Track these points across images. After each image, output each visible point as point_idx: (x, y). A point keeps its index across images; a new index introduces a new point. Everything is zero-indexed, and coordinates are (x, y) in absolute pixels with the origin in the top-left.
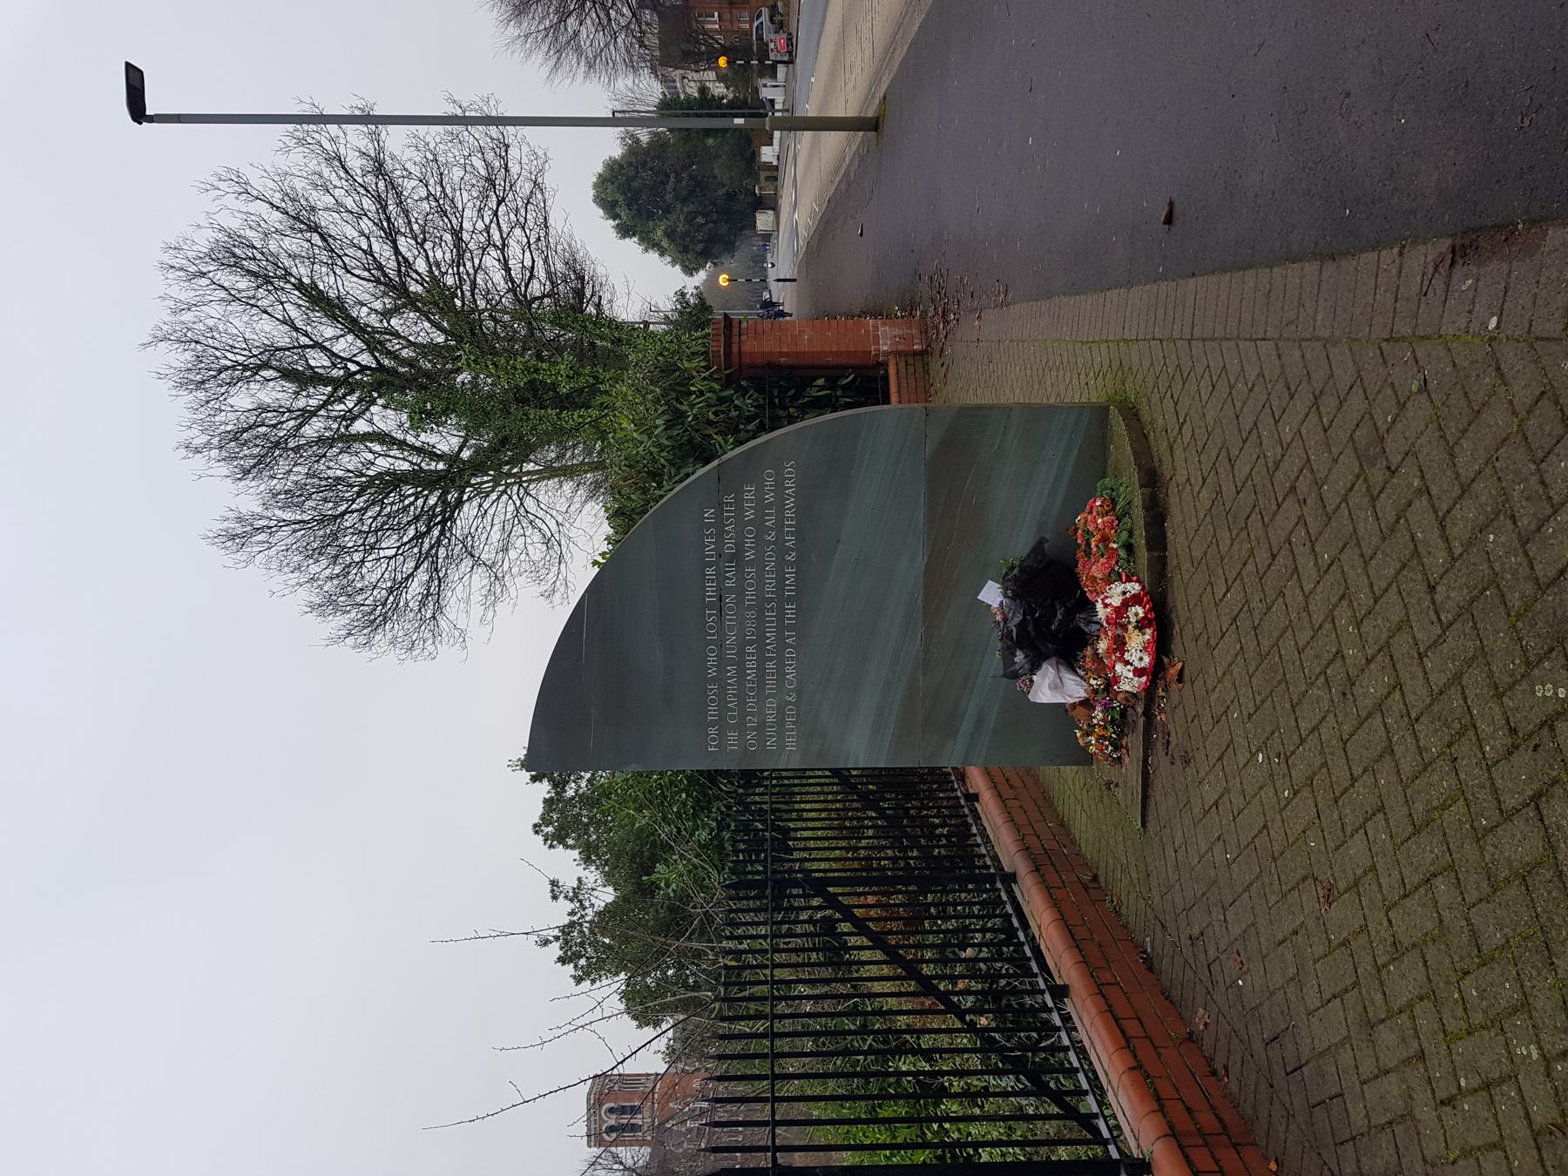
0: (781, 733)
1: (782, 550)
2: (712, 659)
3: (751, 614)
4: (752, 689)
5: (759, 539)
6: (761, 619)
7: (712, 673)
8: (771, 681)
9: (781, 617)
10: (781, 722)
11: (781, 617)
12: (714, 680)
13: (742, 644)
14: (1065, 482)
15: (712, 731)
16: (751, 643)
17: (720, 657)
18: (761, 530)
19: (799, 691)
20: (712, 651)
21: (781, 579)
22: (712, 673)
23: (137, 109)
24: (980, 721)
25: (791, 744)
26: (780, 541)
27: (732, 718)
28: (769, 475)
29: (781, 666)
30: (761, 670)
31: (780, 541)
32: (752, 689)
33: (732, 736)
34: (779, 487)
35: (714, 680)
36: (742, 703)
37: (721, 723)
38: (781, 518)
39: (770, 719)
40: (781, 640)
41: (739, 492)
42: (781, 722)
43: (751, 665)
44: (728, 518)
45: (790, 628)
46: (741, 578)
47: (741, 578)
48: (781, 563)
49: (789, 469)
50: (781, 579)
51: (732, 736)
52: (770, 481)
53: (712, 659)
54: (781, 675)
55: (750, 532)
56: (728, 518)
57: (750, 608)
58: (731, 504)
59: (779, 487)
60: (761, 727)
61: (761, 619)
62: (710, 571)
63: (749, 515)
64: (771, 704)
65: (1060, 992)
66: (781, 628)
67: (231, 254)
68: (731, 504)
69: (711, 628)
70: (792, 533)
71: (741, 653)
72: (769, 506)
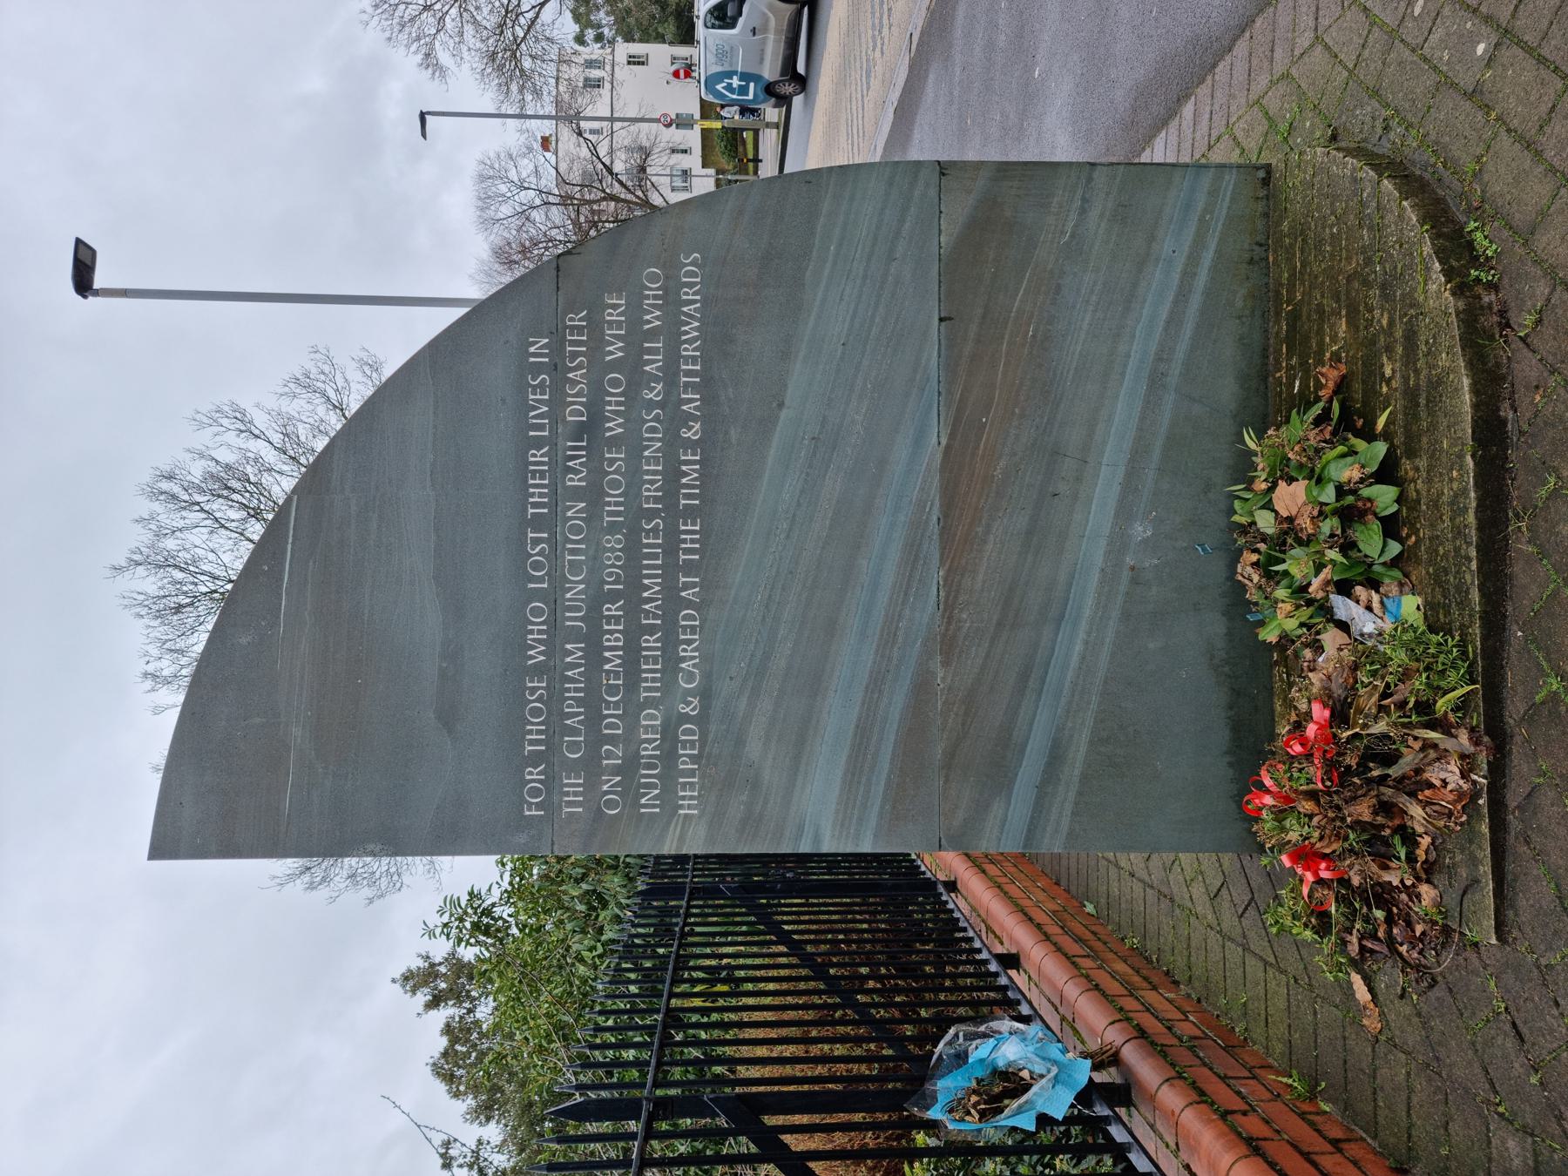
1: (675, 420)
2: (537, 628)
3: (614, 542)
4: (613, 690)
6: (633, 551)
7: (536, 655)
8: (650, 673)
9: (671, 549)
10: (669, 755)
11: (671, 549)
12: (539, 671)
13: (597, 599)
14: (1196, 301)
16: (613, 597)
17: (553, 623)
19: (705, 694)
20: (537, 612)
21: (673, 475)
22: (536, 655)
23: (83, 280)
24: (1056, 757)
26: (670, 403)
27: (574, 747)
28: (653, 278)
31: (670, 403)
33: (573, 784)
34: (671, 300)
35: (539, 671)
36: (594, 719)
37: (548, 757)
39: (648, 751)
40: (671, 591)
41: (596, 309)
42: (669, 755)
43: (614, 639)
44: (575, 355)
45: (689, 568)
46: (597, 472)
48: (673, 443)
50: (673, 475)
51: (573, 784)
52: (653, 289)
54: (671, 662)
55: (615, 383)
56: (575, 355)
57: (613, 528)
58: (580, 330)
59: (671, 300)
60: (630, 767)
63: (615, 351)
64: (651, 719)
67: (224, 483)
68: (580, 330)
69: (537, 566)
71: (594, 617)
72: (653, 334)
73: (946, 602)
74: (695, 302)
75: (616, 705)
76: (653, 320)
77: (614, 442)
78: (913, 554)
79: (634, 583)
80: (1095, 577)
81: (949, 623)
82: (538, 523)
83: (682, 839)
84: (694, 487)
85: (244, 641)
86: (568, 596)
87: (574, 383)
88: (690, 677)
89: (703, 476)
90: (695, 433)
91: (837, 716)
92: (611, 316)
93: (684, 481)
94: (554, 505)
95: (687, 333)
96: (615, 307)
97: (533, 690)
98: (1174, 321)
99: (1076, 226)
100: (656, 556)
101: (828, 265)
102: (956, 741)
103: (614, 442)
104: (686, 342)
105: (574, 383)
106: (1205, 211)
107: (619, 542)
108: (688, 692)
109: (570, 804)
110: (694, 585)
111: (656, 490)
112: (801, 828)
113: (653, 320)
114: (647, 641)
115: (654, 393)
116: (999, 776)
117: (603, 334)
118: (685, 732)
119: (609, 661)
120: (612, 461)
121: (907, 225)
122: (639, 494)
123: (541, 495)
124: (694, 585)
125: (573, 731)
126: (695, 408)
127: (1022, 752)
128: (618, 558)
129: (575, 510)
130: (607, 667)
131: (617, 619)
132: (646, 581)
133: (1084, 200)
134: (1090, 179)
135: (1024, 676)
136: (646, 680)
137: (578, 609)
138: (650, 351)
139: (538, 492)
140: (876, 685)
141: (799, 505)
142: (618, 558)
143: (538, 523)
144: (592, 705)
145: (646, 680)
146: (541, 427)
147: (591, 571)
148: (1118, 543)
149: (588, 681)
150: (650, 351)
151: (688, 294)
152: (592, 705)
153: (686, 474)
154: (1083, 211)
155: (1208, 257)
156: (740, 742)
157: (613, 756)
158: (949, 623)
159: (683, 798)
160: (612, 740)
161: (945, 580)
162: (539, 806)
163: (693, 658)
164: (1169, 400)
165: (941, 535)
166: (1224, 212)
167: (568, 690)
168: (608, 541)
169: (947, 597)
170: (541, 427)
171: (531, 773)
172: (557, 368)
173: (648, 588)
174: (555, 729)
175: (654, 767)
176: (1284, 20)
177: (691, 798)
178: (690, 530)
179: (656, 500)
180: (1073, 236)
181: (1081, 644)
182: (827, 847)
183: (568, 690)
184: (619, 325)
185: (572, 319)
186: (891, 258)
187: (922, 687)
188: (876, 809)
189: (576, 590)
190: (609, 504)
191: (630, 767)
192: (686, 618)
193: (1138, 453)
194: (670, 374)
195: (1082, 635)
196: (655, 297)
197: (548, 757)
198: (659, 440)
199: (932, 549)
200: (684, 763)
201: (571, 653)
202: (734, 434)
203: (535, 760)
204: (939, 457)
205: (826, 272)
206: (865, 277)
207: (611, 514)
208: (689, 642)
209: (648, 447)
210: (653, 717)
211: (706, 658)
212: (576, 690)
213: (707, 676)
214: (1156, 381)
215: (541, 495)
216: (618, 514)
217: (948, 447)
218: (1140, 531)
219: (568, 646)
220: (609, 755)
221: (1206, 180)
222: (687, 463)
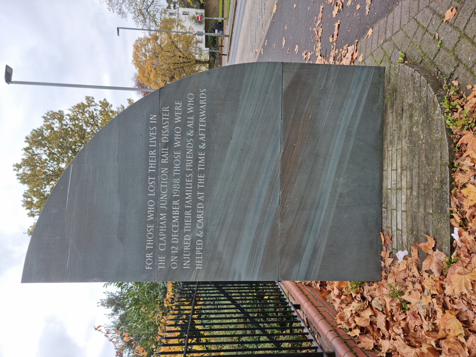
1: (197, 142)
2: (151, 208)
3: (177, 181)
4: (175, 229)
5: (183, 134)
6: (183, 184)
7: (151, 217)
8: (188, 223)
9: (195, 183)
10: (193, 250)
11: (195, 183)
12: (151, 222)
13: (171, 199)
14: (361, 109)
16: (176, 199)
17: (156, 208)
18: (185, 129)
19: (205, 230)
20: (151, 203)
21: (196, 160)
22: (151, 217)
24: (315, 251)
25: (199, 265)
26: (196, 137)
28: (191, 97)
29: (194, 214)
30: (182, 217)
31: (196, 137)
32: (175, 229)
33: (162, 259)
35: (151, 222)
36: (169, 238)
38: (197, 123)
39: (186, 248)
40: (194, 197)
41: (172, 106)
42: (193, 250)
43: (176, 212)
44: (165, 121)
46: (171, 159)
48: (196, 150)
50: (196, 160)
51: (162, 259)
52: (191, 100)
54: (194, 220)
55: (178, 130)
56: (165, 121)
57: (176, 177)
60: (180, 254)
63: (178, 120)
64: (188, 238)
66: (195, 190)
69: (151, 188)
71: (170, 205)
72: (190, 115)
73: (282, 202)
74: (204, 105)
75: (176, 234)
77: (177, 149)
78: (272, 186)
79: (183, 195)
80: (328, 194)
81: (283, 209)
82: (152, 175)
83: (196, 277)
84: (203, 164)
85: (54, 212)
86: (161, 198)
88: (200, 225)
89: (206, 160)
90: (203, 147)
91: (247, 238)
92: (177, 108)
93: (199, 162)
94: (157, 169)
95: (201, 114)
96: (178, 105)
97: (149, 228)
98: (354, 116)
99: (325, 84)
100: (190, 186)
101: (248, 92)
102: (284, 247)
103: (177, 149)
104: (201, 117)
105: (165, 130)
106: (365, 81)
107: (178, 181)
108: (200, 230)
109: (161, 265)
110: (202, 195)
111: (191, 165)
112: (235, 273)
114: (187, 213)
115: (190, 133)
116: (297, 257)
117: (174, 114)
118: (198, 242)
119: (174, 219)
120: (176, 155)
121: (272, 82)
122: (185, 166)
123: (153, 166)
124: (202, 195)
125: (162, 242)
126: (204, 139)
127: (305, 250)
128: (178, 186)
130: (173, 221)
131: (177, 206)
132: (187, 194)
133: (328, 76)
134: (329, 70)
135: (306, 226)
136: (186, 226)
137: (165, 203)
138: (189, 120)
139: (152, 164)
140: (260, 227)
141: (236, 170)
142: (178, 186)
143: (152, 175)
144: (169, 233)
145: (186, 226)
146: (154, 144)
147: (169, 190)
148: (335, 186)
149: (167, 226)
150: (189, 120)
151: (202, 102)
152: (169, 233)
153: (200, 160)
154: (327, 80)
155: (365, 95)
156: (216, 246)
158: (283, 209)
159: (197, 263)
160: (175, 245)
161: (282, 195)
162: (150, 266)
163: (202, 219)
164: (352, 140)
165: (281, 181)
166: (371, 81)
167: (161, 229)
168: (175, 181)
169: (282, 200)
170: (154, 144)
171: (148, 255)
172: (159, 125)
173: (187, 196)
175: (188, 253)
176: (390, 21)
177: (200, 263)
178: (201, 178)
179: (191, 168)
180: (324, 87)
181: (323, 216)
182: (243, 279)
183: (161, 229)
184: (180, 111)
185: (164, 109)
186: (267, 92)
187: (274, 228)
188: (259, 267)
189: (164, 196)
190: (175, 169)
191: (180, 254)
192: (200, 206)
193: (342, 156)
195: (324, 213)
196: (191, 103)
197: (154, 250)
198: (192, 149)
199: (278, 185)
200: (198, 252)
201: (162, 217)
202: (216, 147)
203: (149, 251)
204: (281, 156)
205: (246, 97)
206: (258, 98)
207: (176, 172)
208: (200, 214)
209: (188, 151)
210: (188, 238)
211: (206, 219)
212: (163, 229)
213: (206, 225)
214: (348, 134)
215: (153, 166)
216: (178, 172)
217: (284, 153)
218: (341, 180)
219: (161, 214)
221: (365, 72)
222: (201, 156)
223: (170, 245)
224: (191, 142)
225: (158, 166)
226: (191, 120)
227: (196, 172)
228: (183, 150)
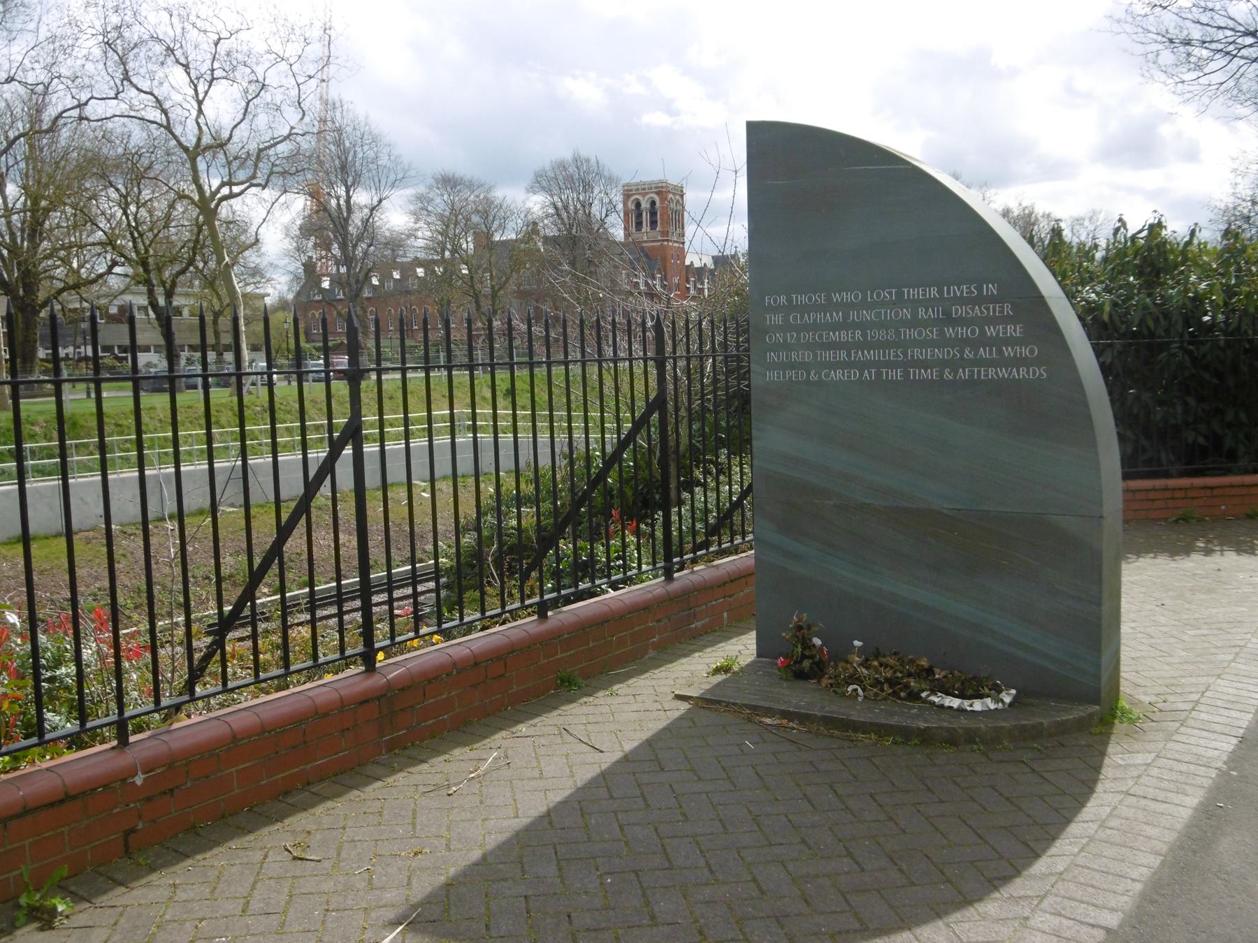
0: (784, 366)
1: (954, 365)
2: (848, 297)
3: (891, 335)
5: (965, 342)
6: (887, 345)
7: (836, 297)
8: (828, 355)
9: (890, 365)
10: (793, 366)
11: (890, 365)
12: (829, 298)
13: (863, 326)
15: (783, 299)
16: (864, 335)
17: (852, 306)
18: (974, 344)
19: (820, 383)
21: (925, 365)
22: (836, 297)
26: (963, 363)
27: (795, 318)
28: (1032, 352)
31: (963, 363)
32: (821, 337)
33: (777, 319)
34: (1019, 362)
35: (829, 298)
36: (806, 328)
42: (793, 366)
43: (843, 336)
44: (988, 309)
45: (879, 374)
46: (925, 324)
47: (925, 324)
48: (943, 364)
49: (1042, 372)
50: (925, 365)
51: (777, 319)
52: (1025, 352)
53: (848, 297)
55: (973, 332)
56: (988, 309)
58: (1002, 312)
59: (1019, 362)
60: (786, 346)
61: (887, 345)
62: (934, 292)
63: (990, 331)
65: (542, 610)
66: (878, 365)
68: (1002, 312)
69: (879, 295)
70: (971, 375)
76: (1008, 351)
77: (941, 333)
87: (973, 310)
103: (941, 333)
105: (973, 310)
108: (820, 377)
113: (1008, 351)
115: (968, 353)
129: (906, 313)
138: (991, 351)
146: (949, 293)
150: (991, 351)
152: (815, 327)
157: (791, 337)
170: (949, 293)
172: (980, 300)
174: (804, 309)
178: (896, 375)
179: (912, 356)
189: (867, 315)
194: (979, 362)
197: (791, 307)
203: (789, 300)
220: (792, 336)
223: (799, 329)
224: (955, 355)
225: (915, 304)
226: (991, 354)
227: (906, 365)
228: (943, 342)
